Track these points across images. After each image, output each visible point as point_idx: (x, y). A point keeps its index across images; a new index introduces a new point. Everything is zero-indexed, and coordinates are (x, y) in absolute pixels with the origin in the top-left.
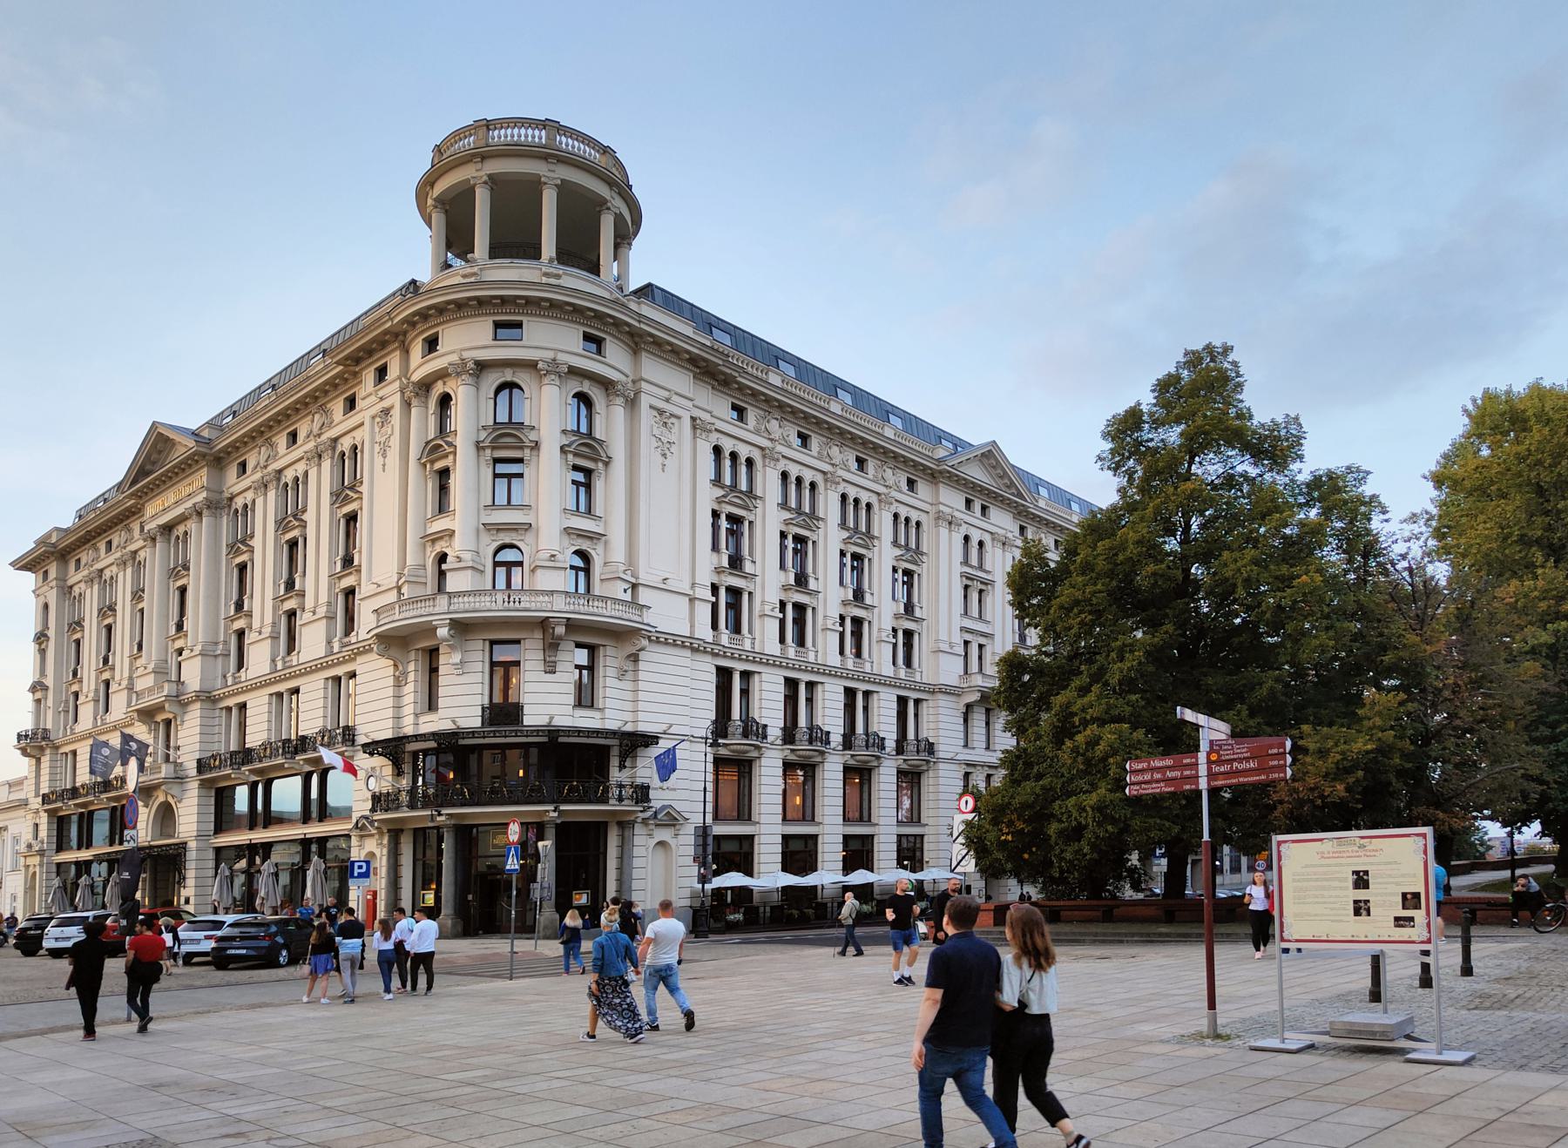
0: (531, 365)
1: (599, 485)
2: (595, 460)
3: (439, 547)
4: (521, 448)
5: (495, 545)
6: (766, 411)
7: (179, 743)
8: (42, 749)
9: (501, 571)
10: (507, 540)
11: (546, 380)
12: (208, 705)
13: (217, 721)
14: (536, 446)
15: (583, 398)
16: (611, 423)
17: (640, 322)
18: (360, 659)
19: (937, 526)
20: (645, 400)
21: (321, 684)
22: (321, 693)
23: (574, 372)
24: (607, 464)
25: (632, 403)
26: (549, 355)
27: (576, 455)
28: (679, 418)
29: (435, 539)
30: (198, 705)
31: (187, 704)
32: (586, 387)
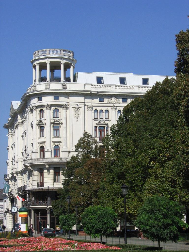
3: (42, 145)
5: (54, 145)
14: (62, 124)
29: (40, 143)
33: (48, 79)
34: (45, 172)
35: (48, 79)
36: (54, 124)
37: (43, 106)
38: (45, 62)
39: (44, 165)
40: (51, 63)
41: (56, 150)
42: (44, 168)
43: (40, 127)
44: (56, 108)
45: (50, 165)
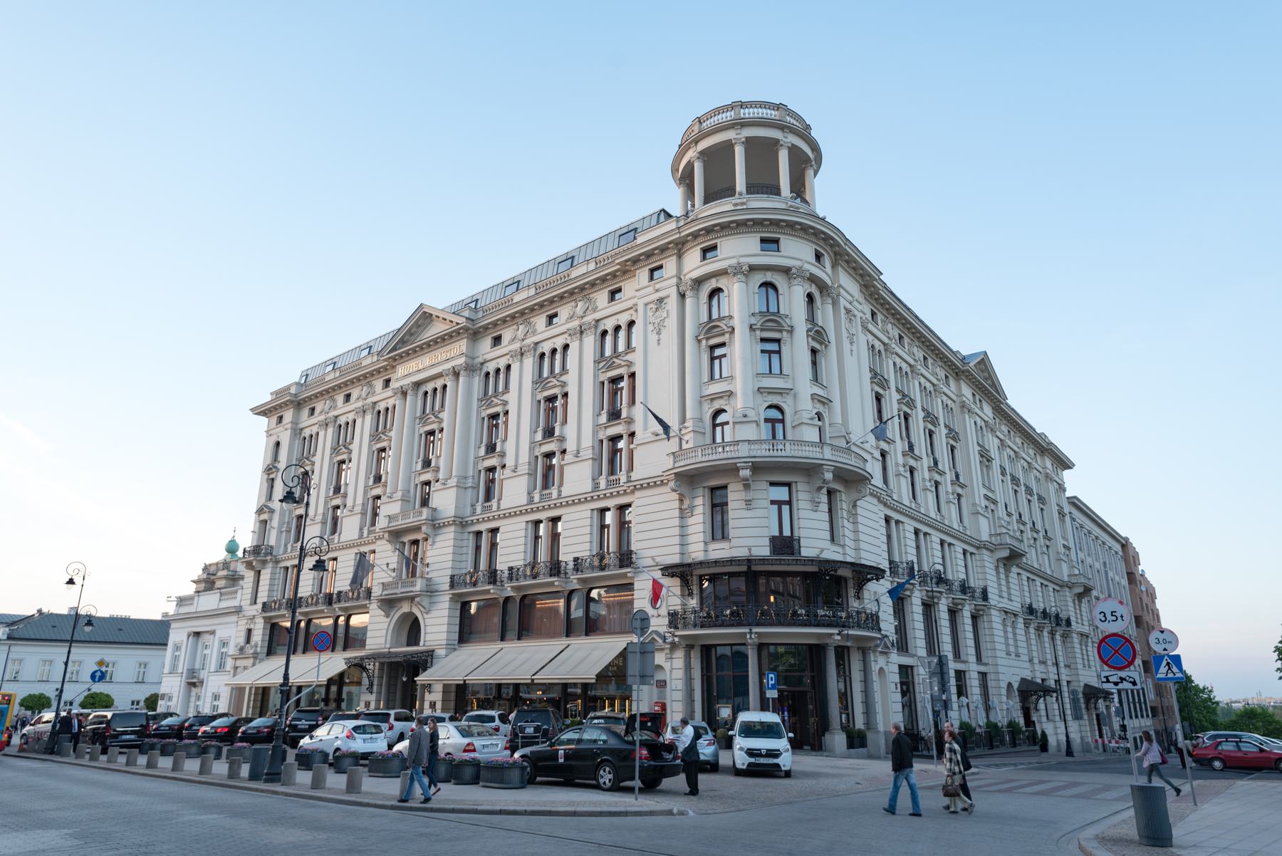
0: (786, 271)
1: (822, 362)
2: (821, 343)
3: (717, 405)
4: (781, 331)
5: (767, 404)
6: (885, 316)
7: (428, 561)
8: (264, 562)
9: (770, 425)
10: (775, 402)
11: (795, 282)
12: (459, 529)
13: (465, 543)
14: (791, 331)
15: (810, 297)
16: (825, 313)
17: (845, 244)
18: (638, 494)
19: (963, 412)
20: (843, 302)
21: (588, 514)
22: (588, 522)
23: (813, 279)
24: (826, 346)
25: (835, 303)
26: (798, 263)
27: (813, 339)
28: (855, 316)
30: (452, 529)
31: (440, 527)
32: (814, 290)
33: (740, 184)
34: (735, 496)
35: (740, 184)
36: (762, 330)
37: (723, 273)
38: (731, 140)
39: (732, 470)
40: (750, 143)
41: (776, 420)
42: (730, 488)
43: (713, 348)
44: (769, 277)
45: (758, 468)
